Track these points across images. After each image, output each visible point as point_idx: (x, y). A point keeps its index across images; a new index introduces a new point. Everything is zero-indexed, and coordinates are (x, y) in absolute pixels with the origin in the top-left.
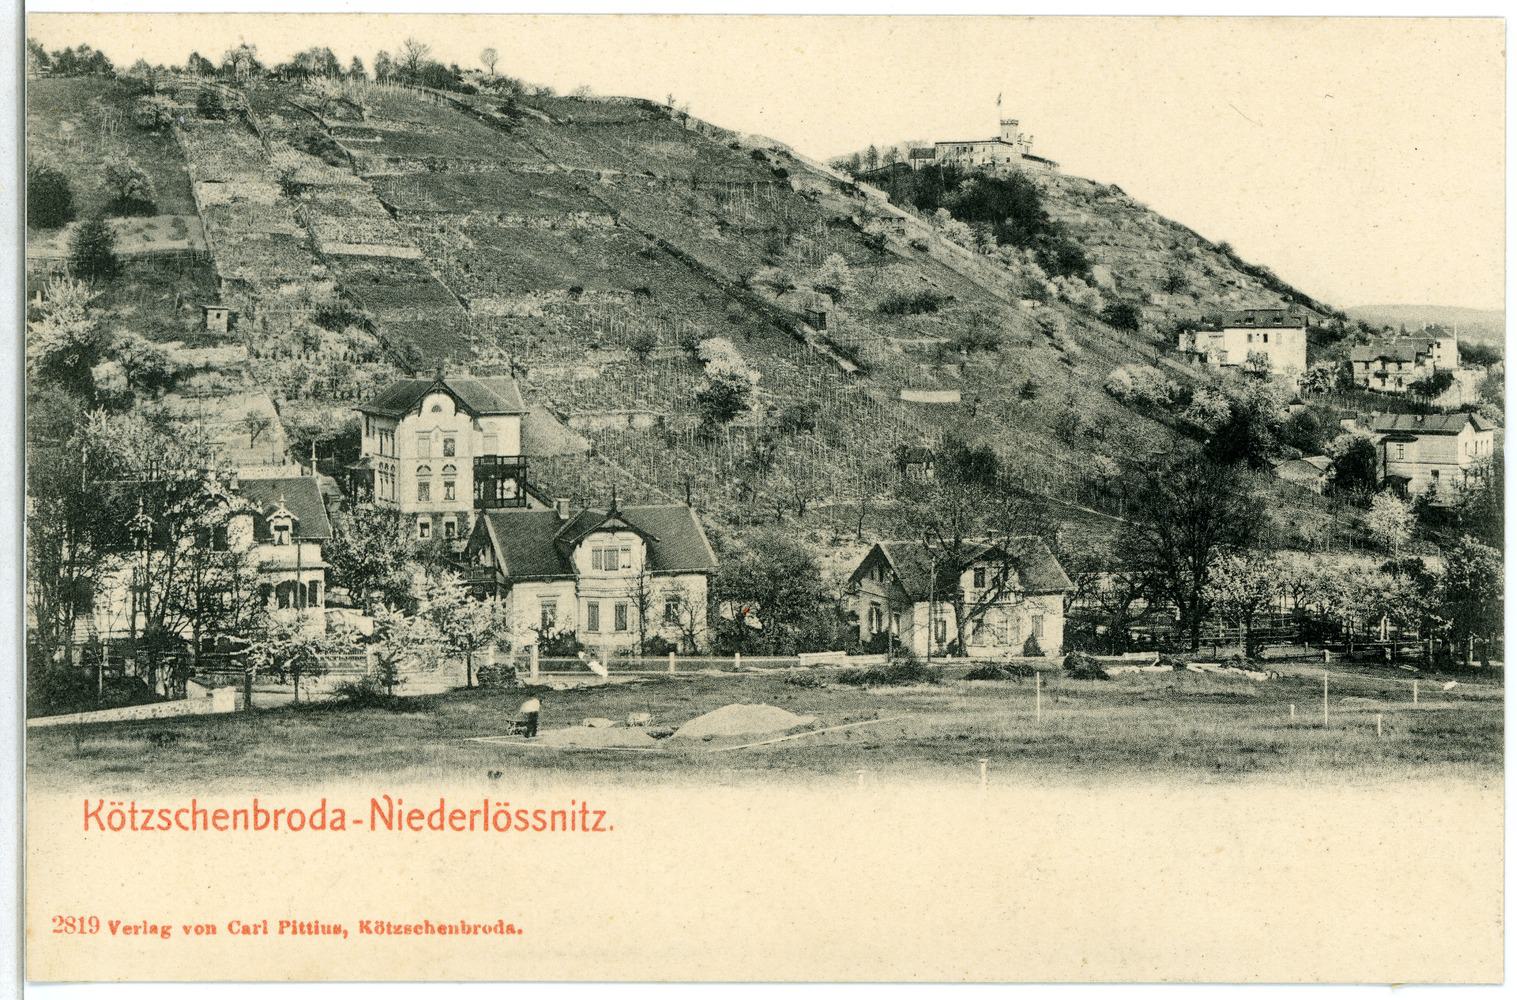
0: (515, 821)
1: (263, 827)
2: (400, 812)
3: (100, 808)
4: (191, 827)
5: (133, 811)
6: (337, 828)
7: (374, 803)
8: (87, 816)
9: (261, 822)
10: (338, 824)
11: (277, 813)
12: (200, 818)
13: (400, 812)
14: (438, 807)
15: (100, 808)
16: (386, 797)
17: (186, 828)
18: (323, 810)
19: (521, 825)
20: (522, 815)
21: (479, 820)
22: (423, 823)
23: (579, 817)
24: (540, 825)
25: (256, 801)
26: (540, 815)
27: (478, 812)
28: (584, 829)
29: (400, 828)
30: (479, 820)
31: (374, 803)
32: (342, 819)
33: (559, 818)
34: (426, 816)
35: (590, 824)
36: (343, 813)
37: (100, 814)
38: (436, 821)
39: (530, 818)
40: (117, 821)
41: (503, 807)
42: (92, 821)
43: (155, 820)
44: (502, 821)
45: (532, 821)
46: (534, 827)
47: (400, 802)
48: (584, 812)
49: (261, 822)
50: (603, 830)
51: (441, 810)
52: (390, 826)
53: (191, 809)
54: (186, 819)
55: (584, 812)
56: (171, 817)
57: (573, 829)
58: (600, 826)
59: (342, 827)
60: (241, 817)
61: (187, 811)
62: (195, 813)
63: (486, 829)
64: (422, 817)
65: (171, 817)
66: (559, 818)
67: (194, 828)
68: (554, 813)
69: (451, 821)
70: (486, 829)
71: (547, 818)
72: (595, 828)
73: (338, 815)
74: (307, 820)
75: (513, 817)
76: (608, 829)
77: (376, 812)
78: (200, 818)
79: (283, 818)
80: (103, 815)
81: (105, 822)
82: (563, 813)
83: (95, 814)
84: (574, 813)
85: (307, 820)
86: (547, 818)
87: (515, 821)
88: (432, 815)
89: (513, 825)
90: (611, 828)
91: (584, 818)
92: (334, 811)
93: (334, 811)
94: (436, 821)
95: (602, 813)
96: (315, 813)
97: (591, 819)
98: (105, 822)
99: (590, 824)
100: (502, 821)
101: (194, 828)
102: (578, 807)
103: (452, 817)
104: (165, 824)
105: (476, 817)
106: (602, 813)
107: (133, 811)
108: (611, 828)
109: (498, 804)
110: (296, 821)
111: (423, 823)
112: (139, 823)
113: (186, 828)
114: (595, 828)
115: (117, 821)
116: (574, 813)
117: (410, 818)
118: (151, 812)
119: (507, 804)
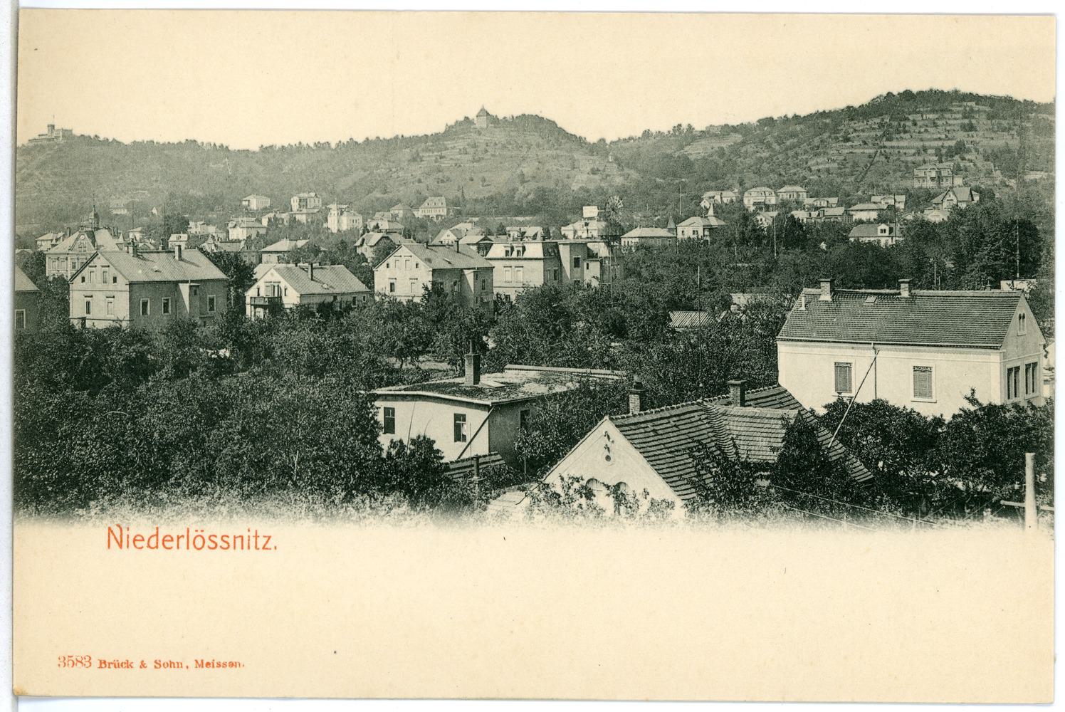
0: (208, 543)
2: (128, 536)
7: (109, 528)
13: (128, 536)
14: (155, 533)
16: (118, 526)
19: (213, 545)
21: (183, 541)
22: (144, 544)
23: (253, 540)
24: (225, 545)
26: (225, 539)
27: (183, 536)
30: (183, 541)
31: (109, 528)
33: (238, 540)
34: (146, 539)
35: (260, 545)
38: (153, 543)
39: (220, 543)
41: (199, 533)
44: (199, 542)
45: (220, 543)
46: (221, 547)
48: (256, 536)
51: (157, 535)
52: (121, 546)
55: (256, 536)
57: (249, 547)
58: (266, 547)
63: (188, 548)
64: (143, 540)
66: (238, 540)
68: (235, 537)
69: (163, 544)
70: (188, 548)
71: (231, 541)
72: (264, 548)
75: (206, 539)
76: (273, 548)
77: (112, 537)
82: (242, 537)
84: (249, 537)
86: (231, 541)
87: (208, 543)
88: (149, 540)
89: (206, 545)
90: (275, 548)
91: (256, 539)
94: (153, 543)
97: (261, 542)
99: (260, 545)
100: (199, 542)
103: (164, 540)
105: (181, 540)
106: (269, 537)
108: (275, 548)
109: (197, 531)
111: (144, 544)
114: (264, 548)
116: (249, 537)
117: (135, 540)
119: (202, 531)
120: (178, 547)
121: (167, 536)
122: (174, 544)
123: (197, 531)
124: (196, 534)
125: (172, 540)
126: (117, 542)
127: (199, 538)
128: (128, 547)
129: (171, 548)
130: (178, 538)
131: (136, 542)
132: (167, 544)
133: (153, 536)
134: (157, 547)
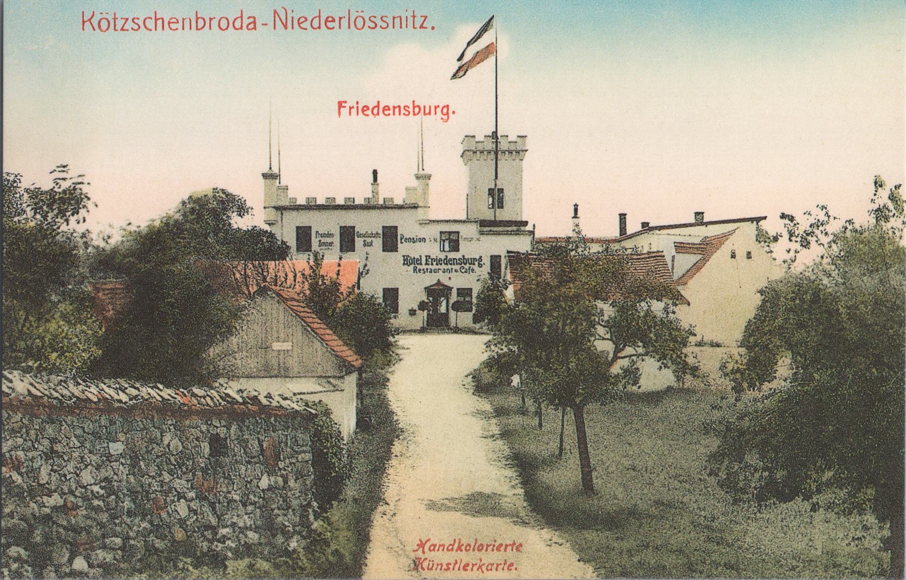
0: (368, 23)
1: (199, 29)
3: (91, 18)
4: (153, 29)
5: (115, 19)
6: (252, 29)
7: (275, 12)
8: (84, 22)
9: (200, 26)
10: (252, 26)
11: (211, 19)
12: (159, 22)
13: (293, 17)
15: (91, 18)
17: (151, 30)
18: (242, 17)
19: (373, 25)
20: (372, 19)
21: (344, 22)
23: (410, 20)
24: (384, 25)
25: (197, 12)
28: (414, 27)
29: (293, 28)
30: (344, 22)
31: (275, 12)
32: (254, 23)
33: (397, 21)
34: (309, 19)
35: (418, 25)
36: (254, 18)
37: (92, 20)
38: (316, 24)
39: (380, 23)
40: (104, 24)
42: (87, 24)
43: (129, 25)
44: (360, 23)
45: (380, 23)
47: (293, 11)
48: (414, 17)
49: (200, 26)
50: (426, 28)
51: (320, 16)
52: (286, 27)
53: (154, 18)
54: (150, 24)
56: (141, 22)
59: (255, 28)
60: (187, 22)
61: (151, 18)
62: (156, 20)
63: (349, 27)
65: (141, 22)
66: (397, 21)
67: (156, 29)
68: (394, 18)
69: (326, 24)
70: (349, 27)
73: (252, 20)
74: (231, 23)
77: (277, 18)
78: (159, 22)
79: (215, 23)
80: (95, 21)
81: (96, 26)
82: (400, 17)
83: (90, 20)
85: (231, 23)
87: (368, 23)
92: (249, 18)
93: (249, 18)
94: (316, 24)
95: (426, 17)
96: (235, 19)
98: (96, 26)
99: (418, 25)
100: (360, 23)
101: (156, 29)
102: (410, 14)
103: (326, 21)
104: (136, 27)
106: (426, 17)
107: (115, 19)
110: (224, 24)
112: (119, 27)
113: (151, 30)
114: (422, 27)
115: (104, 24)
118: (127, 19)
120: (340, 28)
121: (328, 17)
122: (336, 24)
123: (357, 12)
124: (357, 14)
125: (334, 21)
126: (283, 23)
127: (361, 19)
128: (293, 28)
129: (333, 28)
130: (340, 18)
131: (301, 25)
132: (330, 25)
133: (315, 17)
134: (319, 28)
